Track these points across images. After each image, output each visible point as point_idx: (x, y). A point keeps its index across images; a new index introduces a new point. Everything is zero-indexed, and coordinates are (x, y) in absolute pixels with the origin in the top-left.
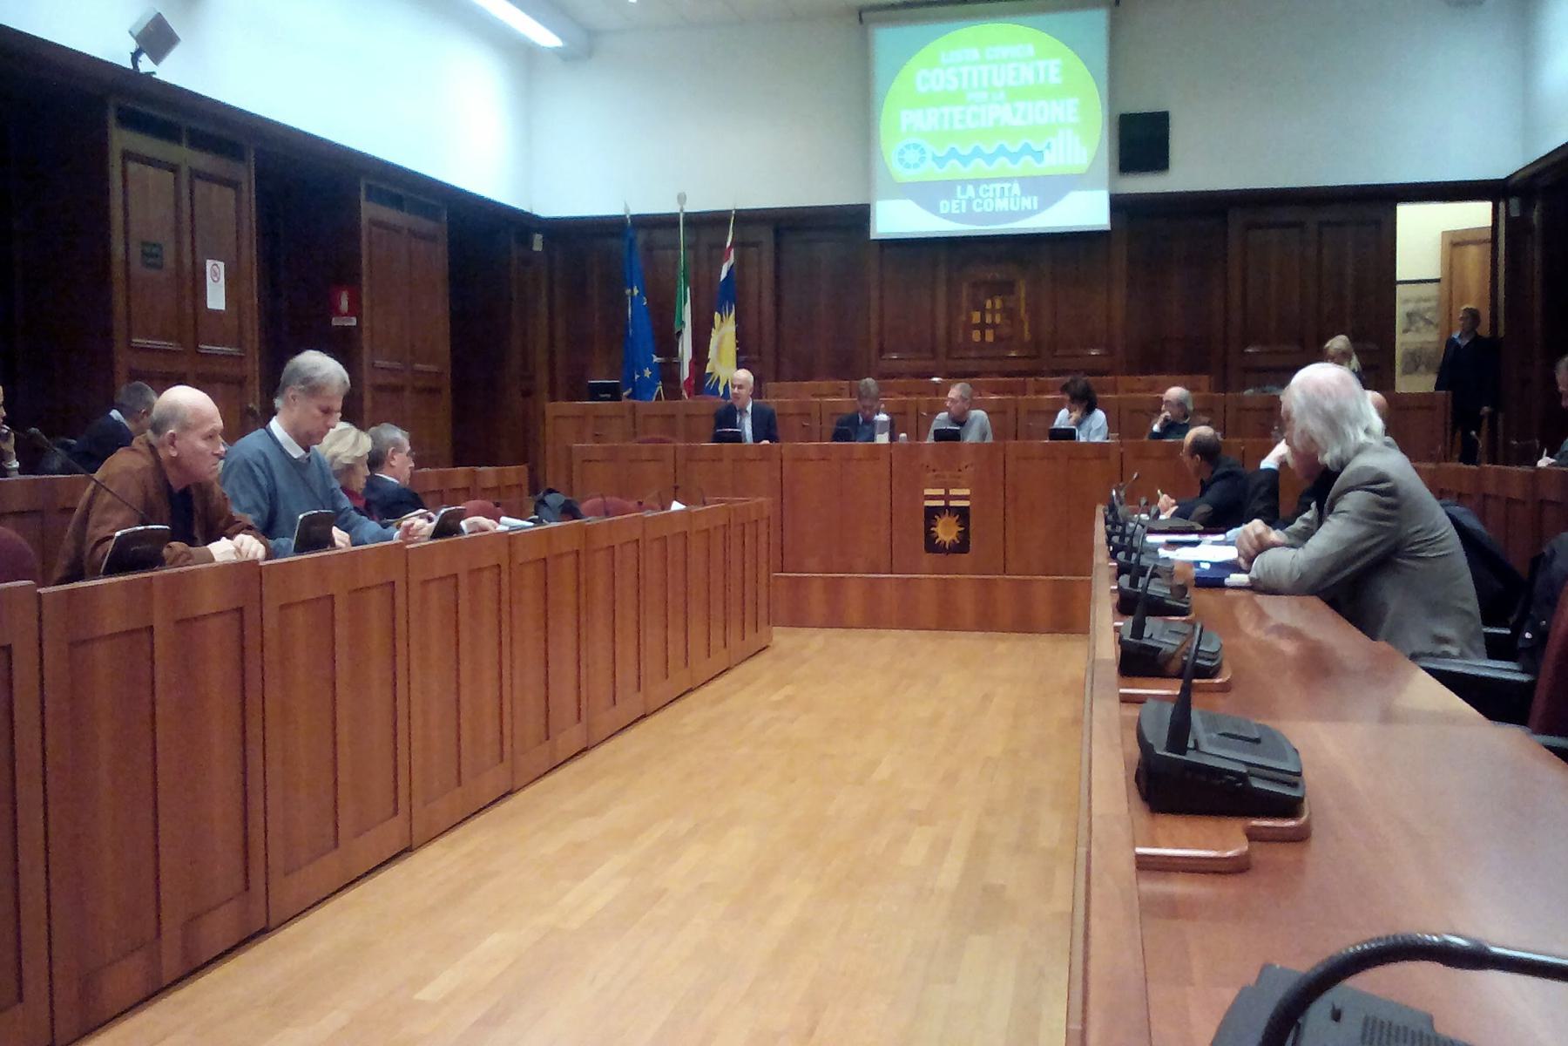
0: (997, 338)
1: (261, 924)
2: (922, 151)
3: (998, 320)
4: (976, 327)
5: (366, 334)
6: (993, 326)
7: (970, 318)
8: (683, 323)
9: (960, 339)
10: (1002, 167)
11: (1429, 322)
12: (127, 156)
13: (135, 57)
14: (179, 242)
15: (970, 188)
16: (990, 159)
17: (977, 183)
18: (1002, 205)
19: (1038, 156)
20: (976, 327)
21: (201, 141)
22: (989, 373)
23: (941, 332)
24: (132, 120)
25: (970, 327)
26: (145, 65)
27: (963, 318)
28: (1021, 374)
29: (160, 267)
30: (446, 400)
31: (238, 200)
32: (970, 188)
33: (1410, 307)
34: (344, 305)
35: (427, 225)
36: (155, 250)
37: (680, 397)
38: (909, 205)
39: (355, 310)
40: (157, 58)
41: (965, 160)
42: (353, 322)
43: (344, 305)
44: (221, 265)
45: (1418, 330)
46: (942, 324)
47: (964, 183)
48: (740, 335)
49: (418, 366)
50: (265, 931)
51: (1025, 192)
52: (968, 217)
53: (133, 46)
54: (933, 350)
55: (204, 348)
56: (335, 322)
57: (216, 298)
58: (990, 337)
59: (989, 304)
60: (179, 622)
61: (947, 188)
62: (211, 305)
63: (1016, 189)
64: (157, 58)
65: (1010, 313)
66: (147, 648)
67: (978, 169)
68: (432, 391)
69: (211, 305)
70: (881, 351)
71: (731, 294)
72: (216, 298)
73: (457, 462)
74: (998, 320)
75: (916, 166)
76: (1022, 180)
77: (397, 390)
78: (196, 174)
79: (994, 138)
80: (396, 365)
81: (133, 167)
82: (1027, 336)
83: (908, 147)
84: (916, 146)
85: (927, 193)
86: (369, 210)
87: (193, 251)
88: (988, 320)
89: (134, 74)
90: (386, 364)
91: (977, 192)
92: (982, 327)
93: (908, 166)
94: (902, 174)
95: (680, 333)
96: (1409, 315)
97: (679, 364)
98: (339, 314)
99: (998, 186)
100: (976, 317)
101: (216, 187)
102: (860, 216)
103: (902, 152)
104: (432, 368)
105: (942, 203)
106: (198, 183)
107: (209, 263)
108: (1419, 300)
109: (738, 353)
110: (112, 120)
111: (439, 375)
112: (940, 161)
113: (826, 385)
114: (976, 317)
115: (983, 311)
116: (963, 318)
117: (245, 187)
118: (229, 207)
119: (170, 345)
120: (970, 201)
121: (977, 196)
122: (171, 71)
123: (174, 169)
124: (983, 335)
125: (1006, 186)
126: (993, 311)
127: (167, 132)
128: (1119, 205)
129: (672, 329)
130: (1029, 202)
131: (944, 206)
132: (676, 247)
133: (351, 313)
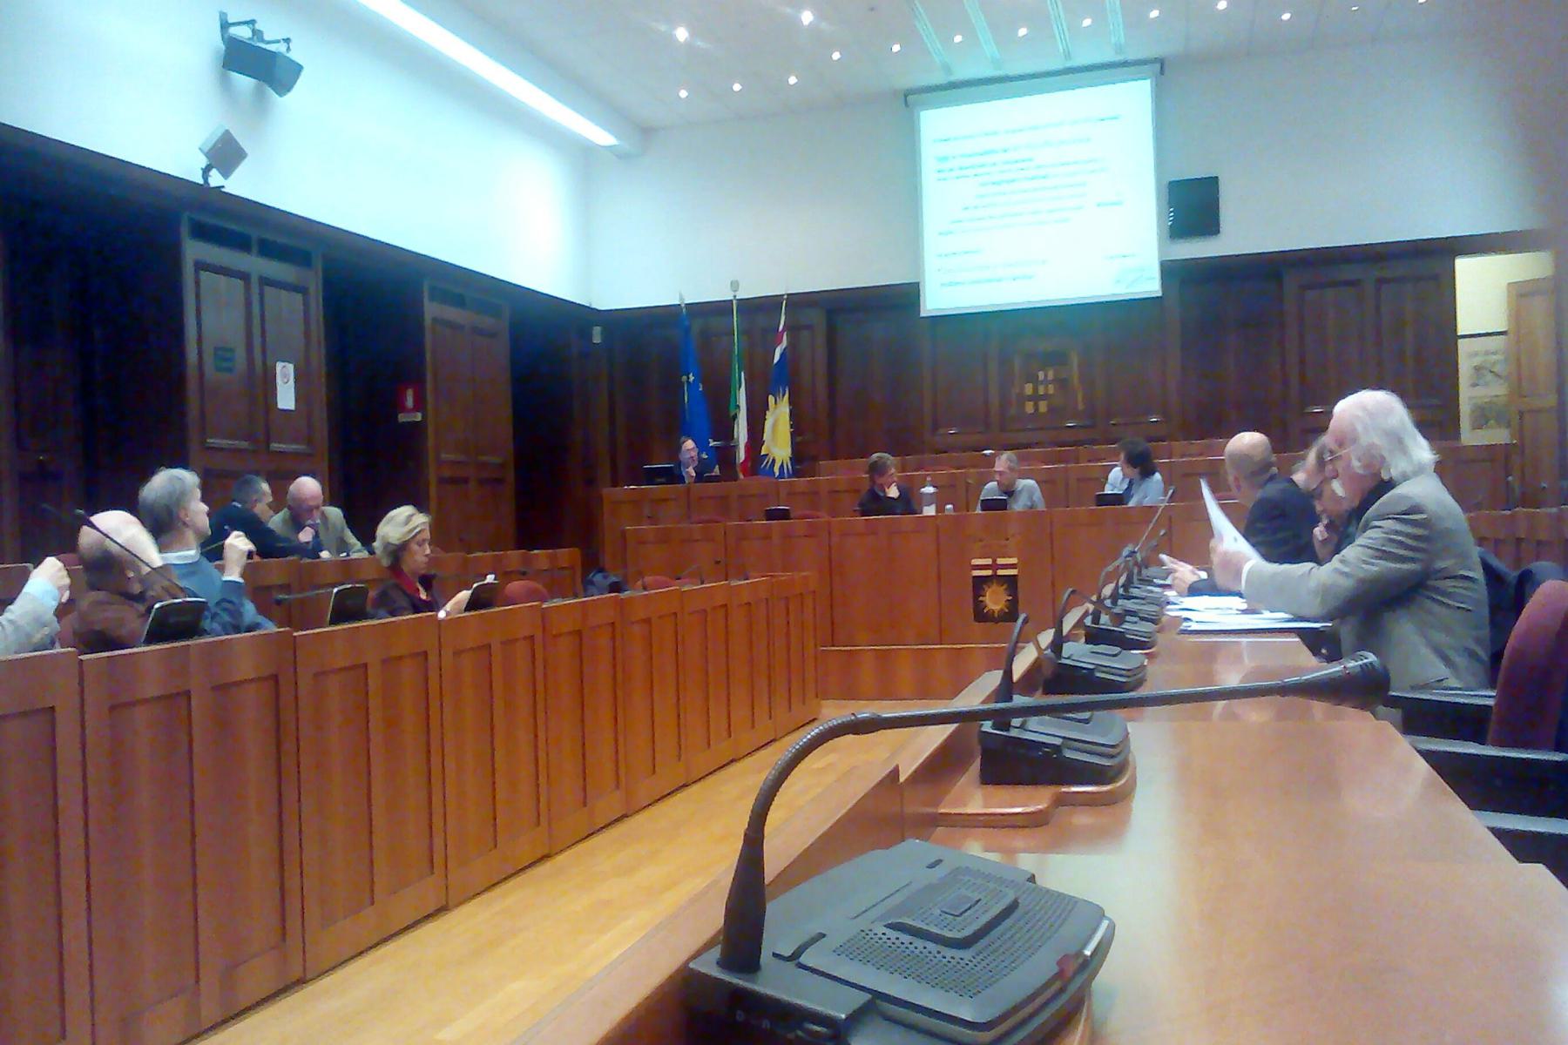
0: (1051, 409)
1: (297, 973)
3: (1051, 391)
4: (1030, 398)
7: (1022, 389)
9: (1013, 411)
11: (1497, 375)
13: (206, 172)
20: (1030, 398)
21: (269, 250)
25: (1023, 399)
26: (215, 179)
29: (230, 370)
30: (509, 490)
31: (306, 304)
33: (1477, 361)
34: (410, 402)
35: (486, 321)
36: (228, 355)
37: (736, 479)
39: (420, 405)
40: (226, 174)
42: (419, 417)
43: (410, 402)
44: (291, 367)
45: (1486, 384)
49: (484, 458)
50: (302, 982)
55: (275, 446)
56: (403, 418)
57: (286, 398)
58: (1043, 406)
59: (1041, 375)
60: (217, 688)
62: (280, 406)
64: (226, 174)
65: (1062, 383)
66: (184, 712)
68: (499, 481)
69: (280, 406)
71: (787, 377)
72: (286, 398)
74: (1051, 391)
77: (466, 481)
78: (265, 282)
79: (1042, 212)
81: (204, 275)
82: (1081, 407)
86: (432, 310)
87: (264, 352)
88: (1041, 392)
89: (204, 189)
92: (1035, 398)
96: (1477, 369)
97: (736, 447)
98: (404, 409)
101: (284, 292)
106: (267, 289)
107: (279, 366)
108: (1487, 353)
111: (502, 466)
115: (1036, 382)
117: (312, 290)
119: (244, 444)
122: (240, 184)
123: (244, 277)
127: (240, 243)
128: (1169, 270)
129: (728, 411)
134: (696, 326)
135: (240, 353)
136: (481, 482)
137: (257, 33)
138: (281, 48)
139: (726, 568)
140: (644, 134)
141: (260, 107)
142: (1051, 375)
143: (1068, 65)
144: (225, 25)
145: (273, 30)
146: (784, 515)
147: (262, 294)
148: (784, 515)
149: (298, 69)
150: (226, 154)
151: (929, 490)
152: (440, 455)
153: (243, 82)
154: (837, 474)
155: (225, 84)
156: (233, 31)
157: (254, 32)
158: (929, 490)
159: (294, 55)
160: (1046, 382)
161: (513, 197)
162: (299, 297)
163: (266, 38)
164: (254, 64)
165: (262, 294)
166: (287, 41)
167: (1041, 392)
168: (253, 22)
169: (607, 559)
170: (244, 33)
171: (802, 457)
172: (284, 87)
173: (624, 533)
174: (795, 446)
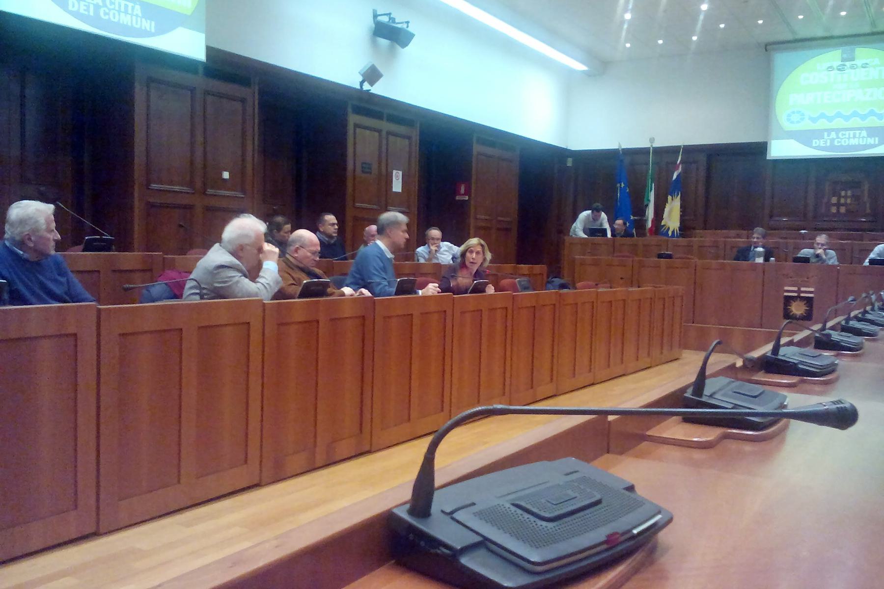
0: (847, 210)
2: (803, 115)
3: (849, 201)
4: (834, 205)
5: (472, 202)
6: (845, 205)
7: (829, 200)
8: (649, 201)
10: (856, 122)
12: (356, 126)
13: (362, 83)
14: (380, 163)
15: (833, 135)
16: (847, 118)
17: (837, 131)
18: (854, 142)
19: (880, 117)
21: (392, 119)
22: (840, 229)
23: (811, 207)
24: (358, 110)
25: (829, 205)
26: (366, 86)
27: (825, 200)
28: (862, 230)
30: (514, 233)
32: (833, 135)
34: (462, 191)
37: (644, 235)
38: (792, 142)
40: (372, 84)
41: (830, 119)
42: (467, 198)
43: (462, 191)
44: (400, 173)
46: (811, 201)
47: (829, 131)
48: (683, 208)
49: (499, 218)
51: (870, 135)
52: (832, 148)
53: (361, 79)
54: (805, 215)
56: (458, 198)
57: (397, 186)
58: (843, 210)
59: (843, 193)
61: (818, 134)
62: (394, 190)
63: (864, 133)
64: (372, 84)
65: (856, 198)
67: (839, 123)
68: (507, 230)
69: (394, 190)
70: (771, 217)
72: (397, 186)
73: (519, 263)
74: (849, 201)
75: (798, 122)
76: (868, 129)
80: (487, 217)
81: (358, 130)
82: (868, 211)
83: (793, 113)
84: (799, 112)
85: (804, 137)
86: (477, 148)
87: (387, 165)
89: (361, 91)
90: (483, 217)
91: (837, 134)
92: (838, 205)
93: (792, 122)
94: (787, 126)
95: (647, 205)
99: (852, 132)
100: (834, 200)
101: (399, 139)
102: (761, 148)
103: (789, 115)
104: (508, 219)
105: (814, 141)
107: (394, 172)
109: (681, 216)
110: (350, 110)
112: (814, 120)
113: (733, 232)
114: (834, 200)
115: (840, 197)
116: (825, 200)
117: (414, 139)
118: (404, 147)
120: (832, 140)
121: (838, 137)
122: (378, 89)
123: (379, 131)
124: (838, 211)
125: (858, 132)
126: (846, 197)
127: (378, 116)
129: (643, 201)
130: (871, 141)
131: (815, 143)
132: (647, 164)
133: (465, 194)
134: (627, 160)
135: (375, 167)
136: (499, 229)
137: (393, 20)
138: (405, 26)
139: (633, 280)
140: (601, 67)
141: (391, 54)
142: (849, 193)
143: (875, 30)
144: (375, 16)
145: (400, 17)
146: (669, 257)
147: (387, 139)
148: (669, 257)
149: (412, 36)
150: (372, 75)
151: (760, 249)
152: (477, 216)
153: (383, 42)
154: (704, 238)
155: (374, 43)
156: (380, 18)
157: (390, 19)
158: (760, 249)
159: (411, 29)
160: (846, 197)
161: (525, 94)
162: (407, 142)
163: (397, 21)
164: (389, 34)
165: (387, 139)
166: (408, 22)
167: (842, 201)
168: (390, 14)
169: (566, 271)
170: (385, 19)
171: (685, 228)
172: (404, 44)
173: (574, 261)
174: (682, 221)
